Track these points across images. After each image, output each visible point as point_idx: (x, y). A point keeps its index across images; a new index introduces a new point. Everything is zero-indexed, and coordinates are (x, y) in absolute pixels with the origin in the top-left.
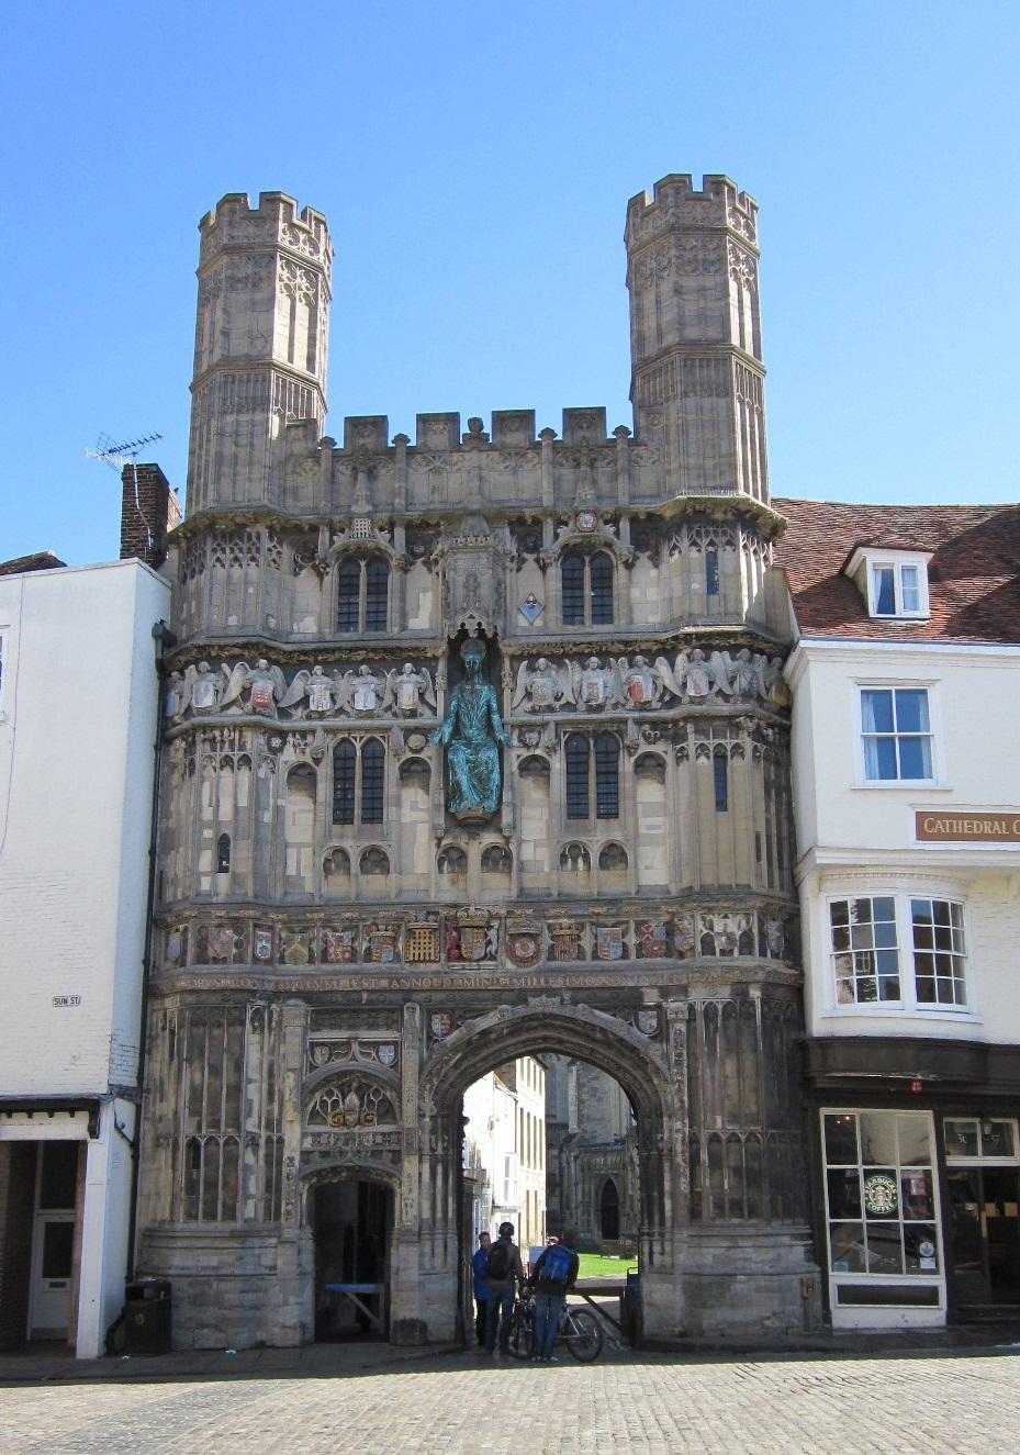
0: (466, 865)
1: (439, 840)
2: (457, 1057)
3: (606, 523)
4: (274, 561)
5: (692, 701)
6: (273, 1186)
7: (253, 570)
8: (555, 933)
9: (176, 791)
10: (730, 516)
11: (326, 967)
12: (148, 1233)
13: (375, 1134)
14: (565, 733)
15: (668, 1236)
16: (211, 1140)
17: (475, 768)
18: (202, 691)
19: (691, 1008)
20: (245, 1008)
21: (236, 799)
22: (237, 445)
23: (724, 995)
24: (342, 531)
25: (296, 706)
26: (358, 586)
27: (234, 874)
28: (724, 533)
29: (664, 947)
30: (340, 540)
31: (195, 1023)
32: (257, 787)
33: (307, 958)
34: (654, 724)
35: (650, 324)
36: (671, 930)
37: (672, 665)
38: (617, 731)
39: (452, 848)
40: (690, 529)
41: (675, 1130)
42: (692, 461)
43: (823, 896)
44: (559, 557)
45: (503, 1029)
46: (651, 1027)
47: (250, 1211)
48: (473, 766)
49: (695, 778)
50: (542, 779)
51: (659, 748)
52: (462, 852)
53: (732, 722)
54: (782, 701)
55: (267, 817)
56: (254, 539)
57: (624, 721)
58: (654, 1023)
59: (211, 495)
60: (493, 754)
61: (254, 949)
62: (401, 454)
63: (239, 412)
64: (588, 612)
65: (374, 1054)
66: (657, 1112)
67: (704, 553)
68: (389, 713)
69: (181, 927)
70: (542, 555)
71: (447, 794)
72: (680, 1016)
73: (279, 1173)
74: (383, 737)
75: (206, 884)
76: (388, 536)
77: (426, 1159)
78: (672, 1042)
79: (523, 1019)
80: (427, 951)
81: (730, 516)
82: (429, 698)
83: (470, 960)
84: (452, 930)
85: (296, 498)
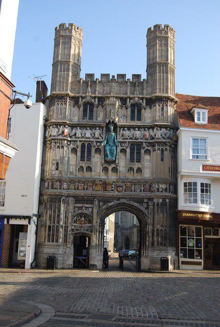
5: (157, 139)
6: (66, 236)
18: (54, 131)
23: (161, 201)
30: (84, 100)
34: (149, 143)
36: (150, 186)
39: (105, 167)
41: (150, 228)
47: (61, 241)
48: (110, 150)
49: (157, 155)
51: (149, 148)
53: (165, 143)
54: (176, 139)
55: (66, 159)
57: (143, 142)
60: (115, 148)
64: (136, 118)
66: (146, 224)
79: (119, 204)
84: (105, 185)
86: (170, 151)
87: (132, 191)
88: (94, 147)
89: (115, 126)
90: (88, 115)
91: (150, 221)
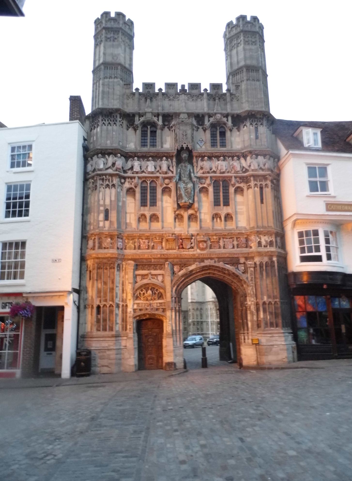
0: (183, 220)
1: (175, 212)
2: (183, 279)
3: (224, 117)
4: (121, 125)
5: (253, 170)
6: (124, 320)
7: (115, 127)
8: (212, 241)
9: (90, 196)
10: (261, 116)
11: (140, 251)
12: (83, 336)
13: (157, 303)
14: (213, 180)
15: (250, 334)
16: (105, 305)
17: (186, 190)
19: (255, 264)
20: (115, 263)
21: (111, 198)
22: (109, 88)
23: (266, 259)
24: (143, 116)
25: (129, 170)
26: (147, 134)
27: (111, 221)
28: (260, 121)
29: (245, 245)
30: (142, 119)
31: (99, 268)
32: (118, 195)
33: (134, 248)
34: (241, 178)
35: (235, 60)
36: (247, 240)
37: (246, 160)
38: (229, 180)
40: (250, 120)
42: (250, 100)
43: (295, 229)
44: (210, 126)
45: (197, 270)
46: (242, 269)
47: (118, 327)
48: (186, 189)
50: (206, 194)
51: (242, 185)
52: (182, 216)
53: (264, 177)
54: (278, 172)
56: (115, 117)
57: (231, 177)
58: (243, 268)
59: (100, 103)
61: (117, 245)
62: (160, 95)
63: (109, 78)
65: (156, 278)
67: (254, 127)
68: (158, 173)
69: (93, 238)
70: (205, 126)
71: (177, 198)
72: (252, 266)
73: (126, 316)
74: (157, 180)
75: (101, 224)
76: (157, 118)
77: (173, 311)
78: (249, 274)
79: (203, 267)
80: (172, 246)
81: (261, 116)
82: (171, 168)
83: (186, 249)
85: (127, 106)
86: (272, 189)
87: (220, 248)
88: (161, 186)
89: (190, 152)
90: (149, 141)
91: (250, 290)
